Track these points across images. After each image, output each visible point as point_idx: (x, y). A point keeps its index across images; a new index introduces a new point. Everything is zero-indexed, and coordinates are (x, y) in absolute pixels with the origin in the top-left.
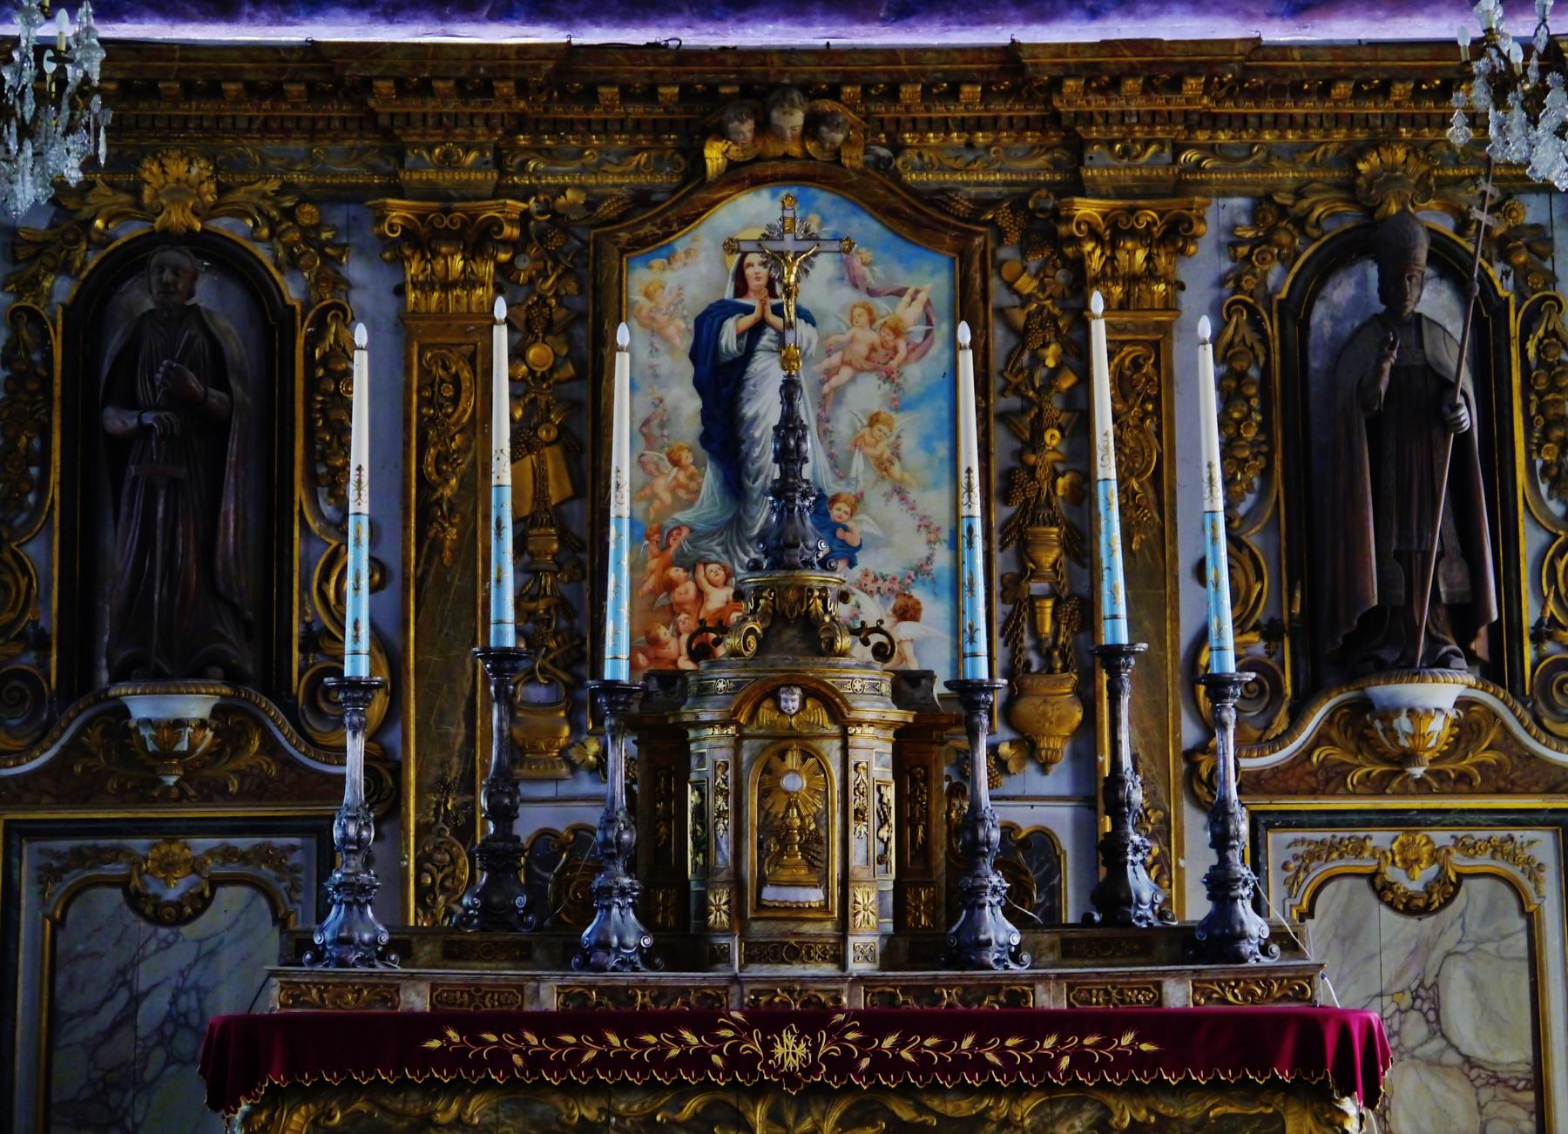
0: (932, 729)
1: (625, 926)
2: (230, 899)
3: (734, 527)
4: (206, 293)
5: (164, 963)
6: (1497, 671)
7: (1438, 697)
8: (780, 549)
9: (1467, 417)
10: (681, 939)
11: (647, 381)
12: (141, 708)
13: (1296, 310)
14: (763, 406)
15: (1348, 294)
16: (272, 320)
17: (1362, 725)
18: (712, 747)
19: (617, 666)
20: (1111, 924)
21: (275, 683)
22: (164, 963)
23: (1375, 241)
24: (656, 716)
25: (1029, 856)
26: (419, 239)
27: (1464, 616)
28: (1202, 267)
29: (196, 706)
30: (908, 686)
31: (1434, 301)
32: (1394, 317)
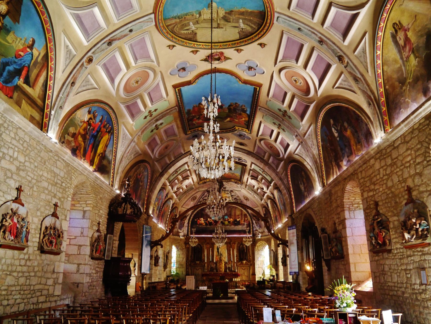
0: (226, 263)
1: (215, 271)
2: (200, 270)
3: (218, 255)
4: (199, 246)
5: (197, 272)
6: (247, 261)
7: (244, 262)
8: (220, 257)
9: (245, 251)
10: (217, 271)
11: (215, 250)
12: (197, 262)
13: (239, 247)
14: (220, 250)
15: (241, 246)
16: (201, 247)
17: (242, 263)
18: (218, 264)
19: (215, 261)
20: (232, 271)
21: (201, 261)
22: (197, 272)
23: (243, 245)
24: (216, 263)
25: (229, 268)
26: (207, 244)
27: (245, 259)
28: (236, 245)
29: (198, 262)
30: (225, 262)
31: (244, 246)
32: (243, 247)
